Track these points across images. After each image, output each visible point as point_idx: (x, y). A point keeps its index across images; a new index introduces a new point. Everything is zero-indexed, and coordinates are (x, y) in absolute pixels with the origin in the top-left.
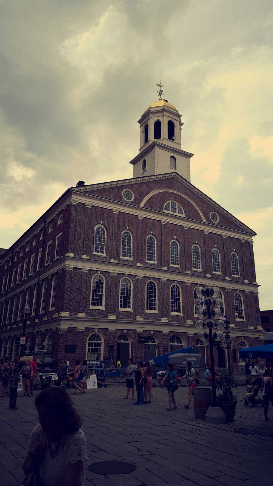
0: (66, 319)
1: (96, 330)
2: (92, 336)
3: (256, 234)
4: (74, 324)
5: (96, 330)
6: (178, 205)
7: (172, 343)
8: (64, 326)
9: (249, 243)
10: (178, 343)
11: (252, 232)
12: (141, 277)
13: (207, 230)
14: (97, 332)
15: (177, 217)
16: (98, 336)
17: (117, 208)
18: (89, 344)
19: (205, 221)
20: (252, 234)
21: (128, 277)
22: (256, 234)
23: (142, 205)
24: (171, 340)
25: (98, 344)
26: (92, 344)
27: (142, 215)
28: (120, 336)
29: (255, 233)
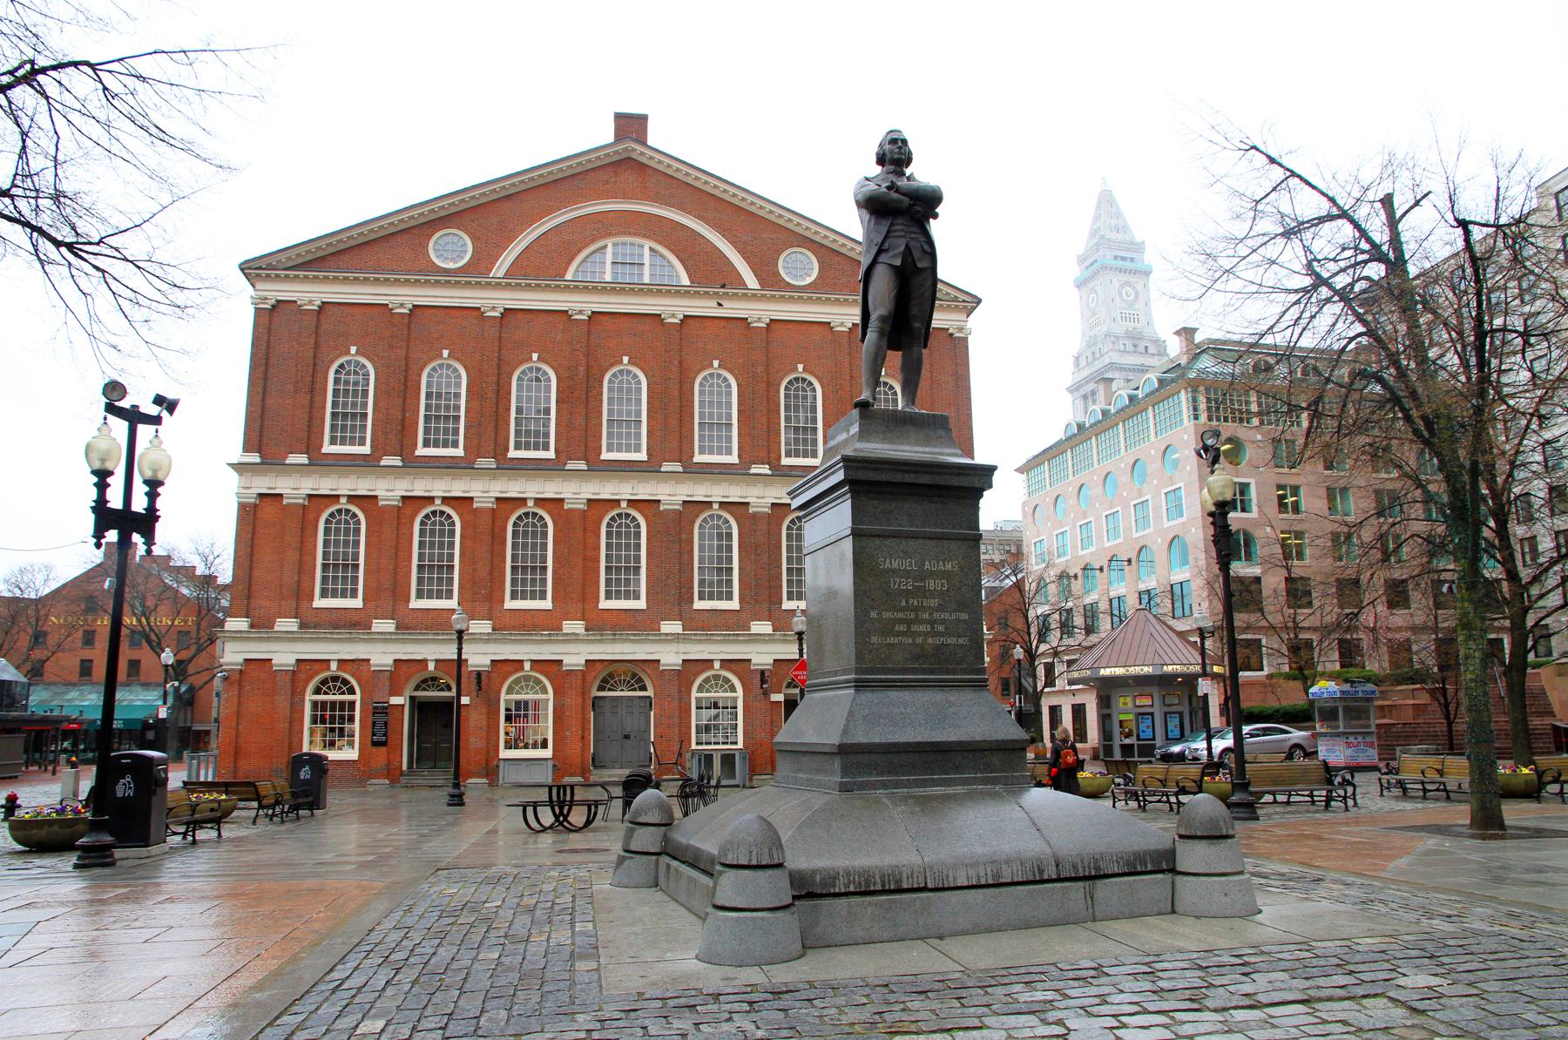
0: (238, 636)
1: (334, 666)
2: (324, 682)
3: (979, 301)
4: (257, 650)
5: (334, 666)
6: (651, 249)
7: (610, 690)
8: (232, 655)
9: (951, 335)
10: (635, 690)
11: (962, 297)
12: (489, 502)
13: (760, 312)
14: (339, 668)
15: (651, 290)
16: (345, 682)
17: (403, 297)
18: (315, 704)
19: (751, 282)
20: (964, 301)
21: (348, 502)
22: (979, 301)
23: (500, 268)
24: (605, 680)
25: (342, 703)
26: (324, 703)
27: (492, 301)
28: (424, 681)
29: (975, 297)
